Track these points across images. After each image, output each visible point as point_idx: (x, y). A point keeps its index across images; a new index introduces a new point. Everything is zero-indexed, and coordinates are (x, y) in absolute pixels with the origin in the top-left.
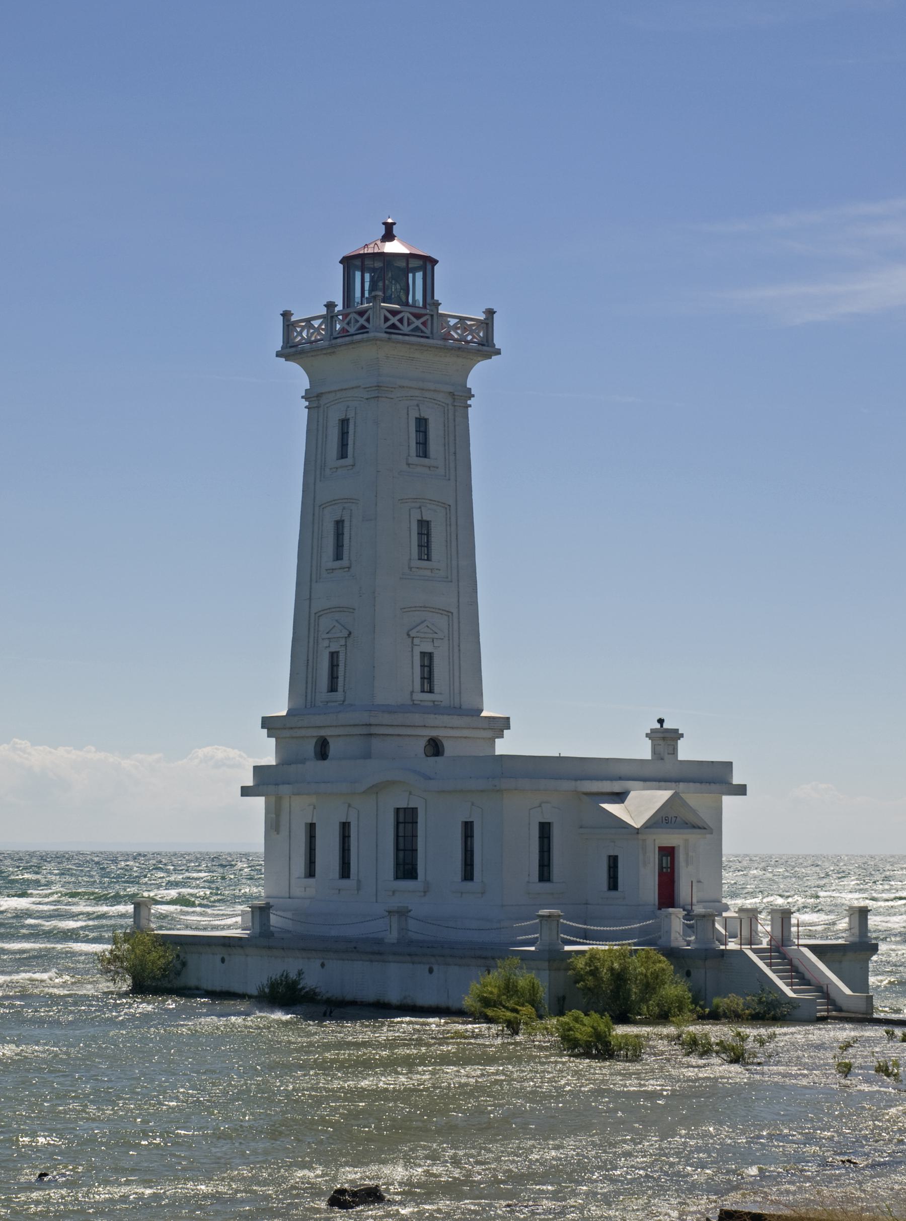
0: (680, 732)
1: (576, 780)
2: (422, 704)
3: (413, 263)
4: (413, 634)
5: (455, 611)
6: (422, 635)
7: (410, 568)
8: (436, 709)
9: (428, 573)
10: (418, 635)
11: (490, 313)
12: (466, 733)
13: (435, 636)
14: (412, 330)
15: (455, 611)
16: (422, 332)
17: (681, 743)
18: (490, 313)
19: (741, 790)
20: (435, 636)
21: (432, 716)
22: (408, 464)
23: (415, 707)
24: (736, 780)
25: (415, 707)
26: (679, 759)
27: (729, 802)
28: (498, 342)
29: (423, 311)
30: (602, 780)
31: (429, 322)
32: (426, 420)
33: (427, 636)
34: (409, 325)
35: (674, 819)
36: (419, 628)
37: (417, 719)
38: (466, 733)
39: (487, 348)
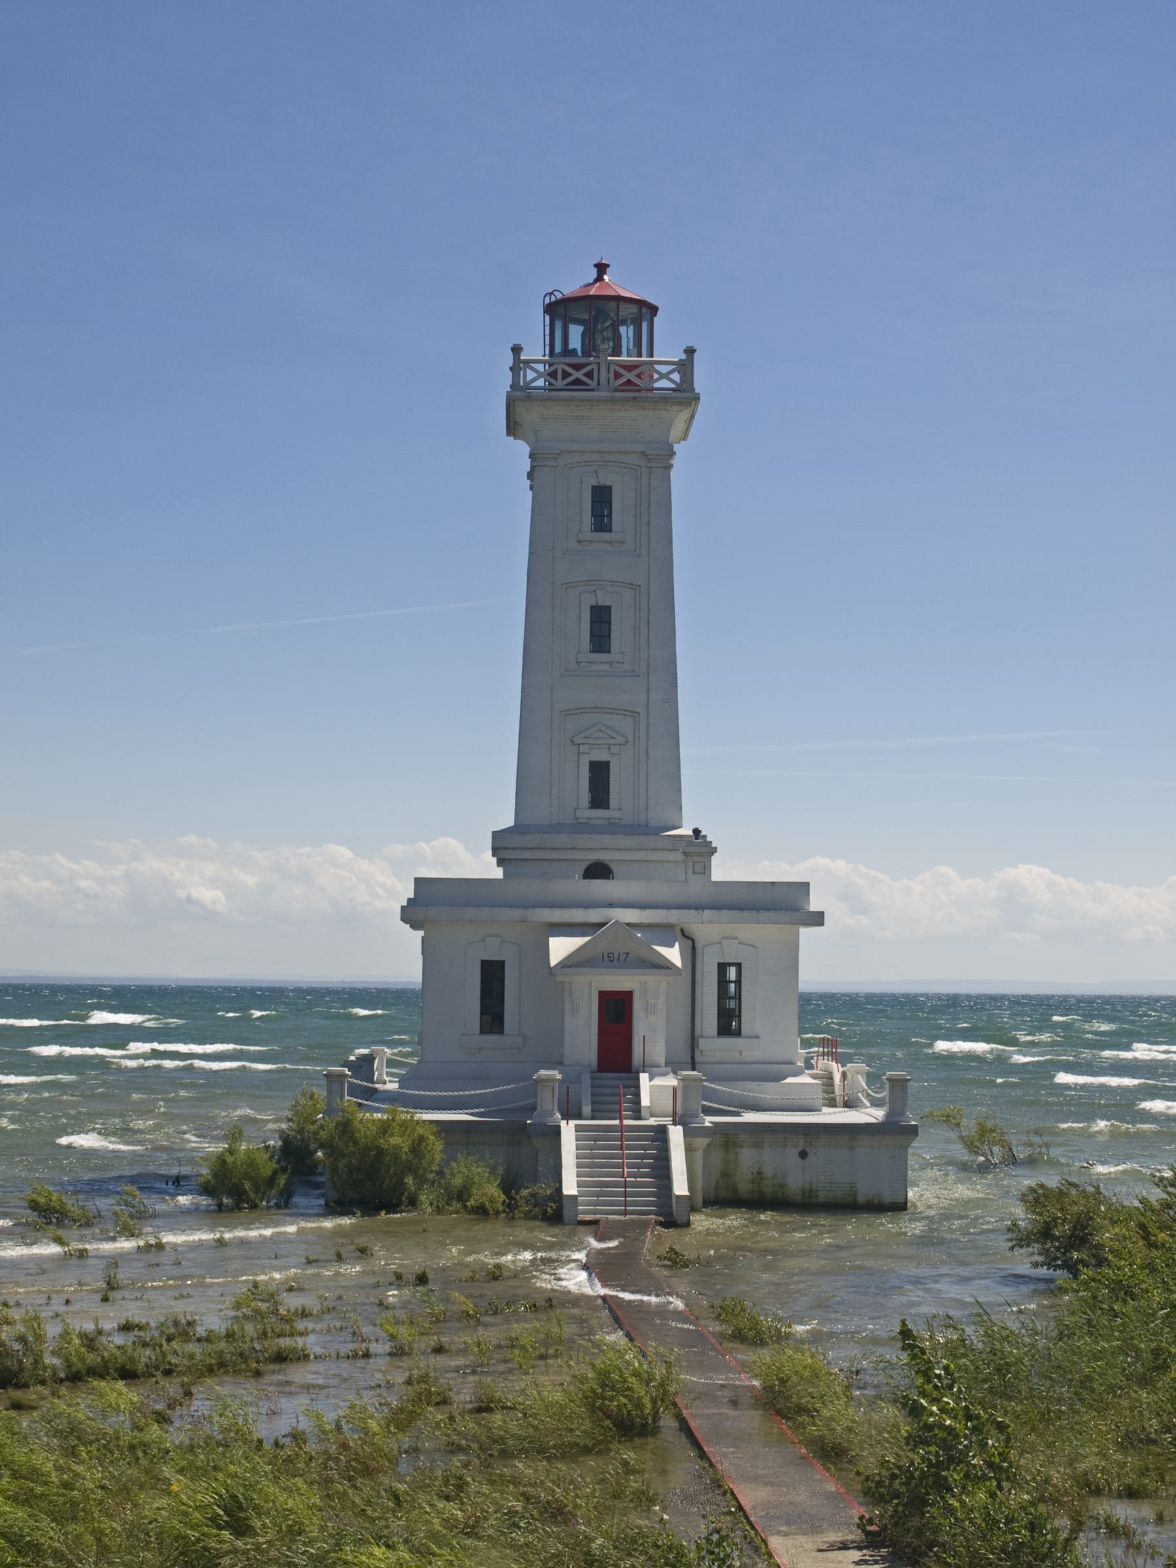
0: (714, 845)
1: (525, 907)
2: (591, 822)
3: (627, 311)
4: (577, 740)
5: (642, 710)
6: (592, 741)
7: (579, 663)
8: (613, 828)
9: (606, 667)
10: (586, 741)
11: (690, 352)
12: (641, 855)
13: (613, 741)
14: (570, 384)
15: (642, 710)
16: (586, 384)
17: (715, 860)
18: (690, 352)
19: (818, 919)
20: (613, 741)
21: (586, 836)
22: (579, 542)
23: (580, 827)
24: (814, 906)
25: (580, 827)
26: (713, 879)
27: (806, 934)
28: (698, 386)
29: (584, 360)
30: (769, 910)
31: (595, 372)
32: (609, 489)
33: (599, 741)
34: (564, 378)
35: (623, 957)
36: (587, 733)
37: (563, 840)
38: (641, 855)
39: (685, 395)
